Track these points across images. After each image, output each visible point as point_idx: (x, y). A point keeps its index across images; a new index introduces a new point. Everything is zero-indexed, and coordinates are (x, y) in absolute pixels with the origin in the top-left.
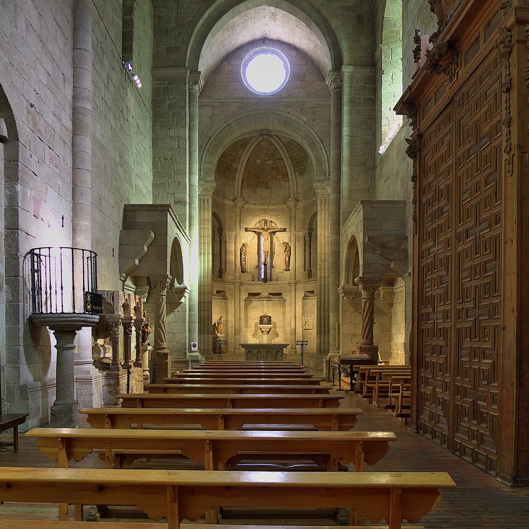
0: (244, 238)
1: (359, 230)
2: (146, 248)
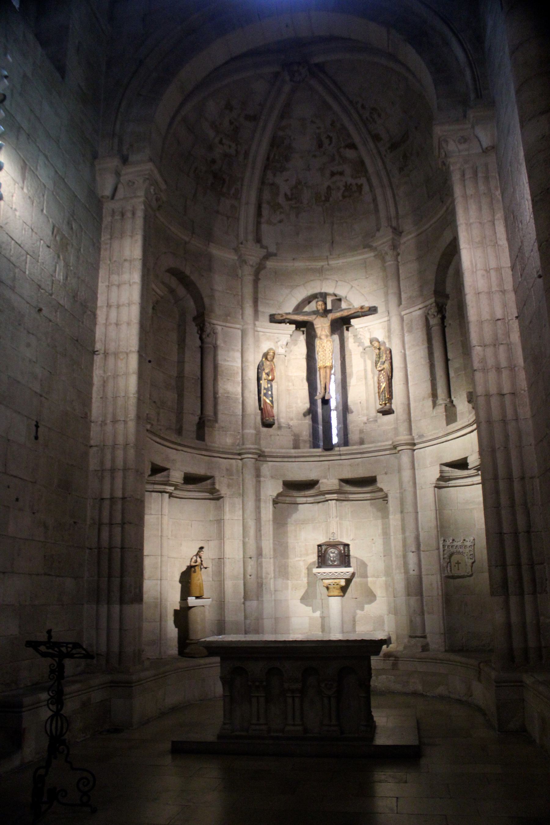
0: (268, 339)
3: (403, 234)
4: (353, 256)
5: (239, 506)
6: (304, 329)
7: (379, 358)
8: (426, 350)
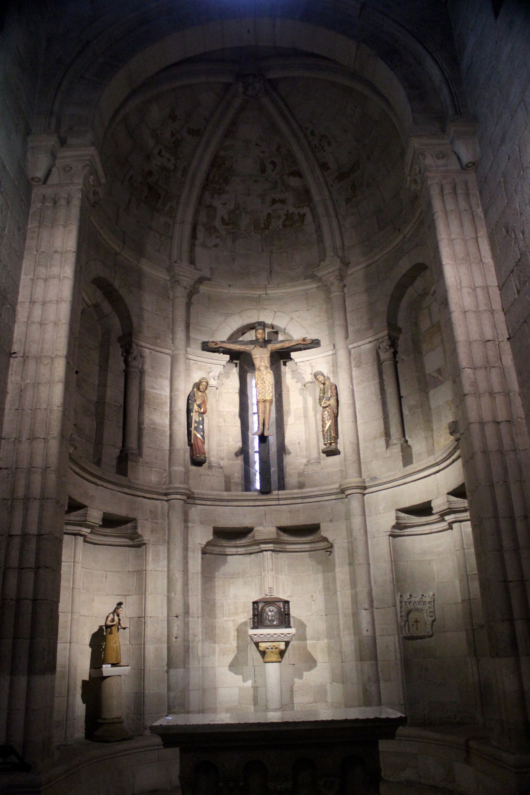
0: (200, 368)
3: (350, 265)
4: (294, 286)
5: (163, 555)
6: (238, 362)
7: (324, 393)
8: (378, 386)
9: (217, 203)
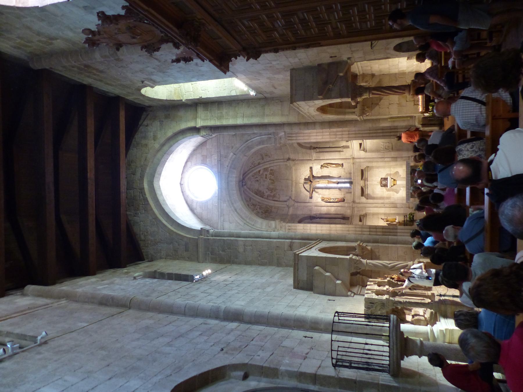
1: (313, 104)
2: (328, 274)
9: (266, 194)
